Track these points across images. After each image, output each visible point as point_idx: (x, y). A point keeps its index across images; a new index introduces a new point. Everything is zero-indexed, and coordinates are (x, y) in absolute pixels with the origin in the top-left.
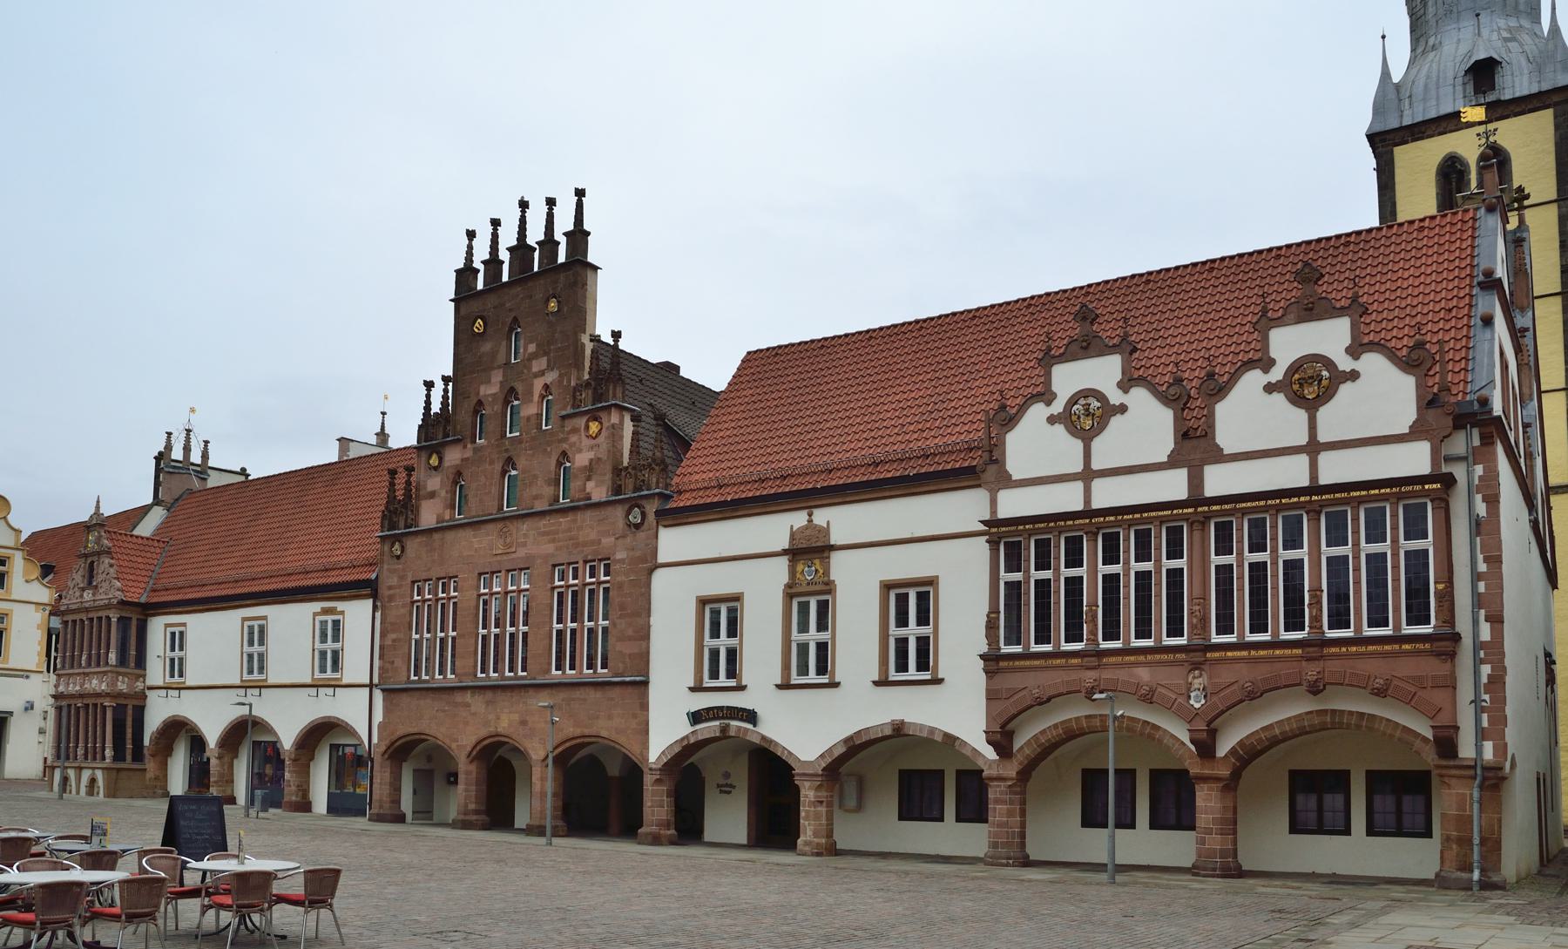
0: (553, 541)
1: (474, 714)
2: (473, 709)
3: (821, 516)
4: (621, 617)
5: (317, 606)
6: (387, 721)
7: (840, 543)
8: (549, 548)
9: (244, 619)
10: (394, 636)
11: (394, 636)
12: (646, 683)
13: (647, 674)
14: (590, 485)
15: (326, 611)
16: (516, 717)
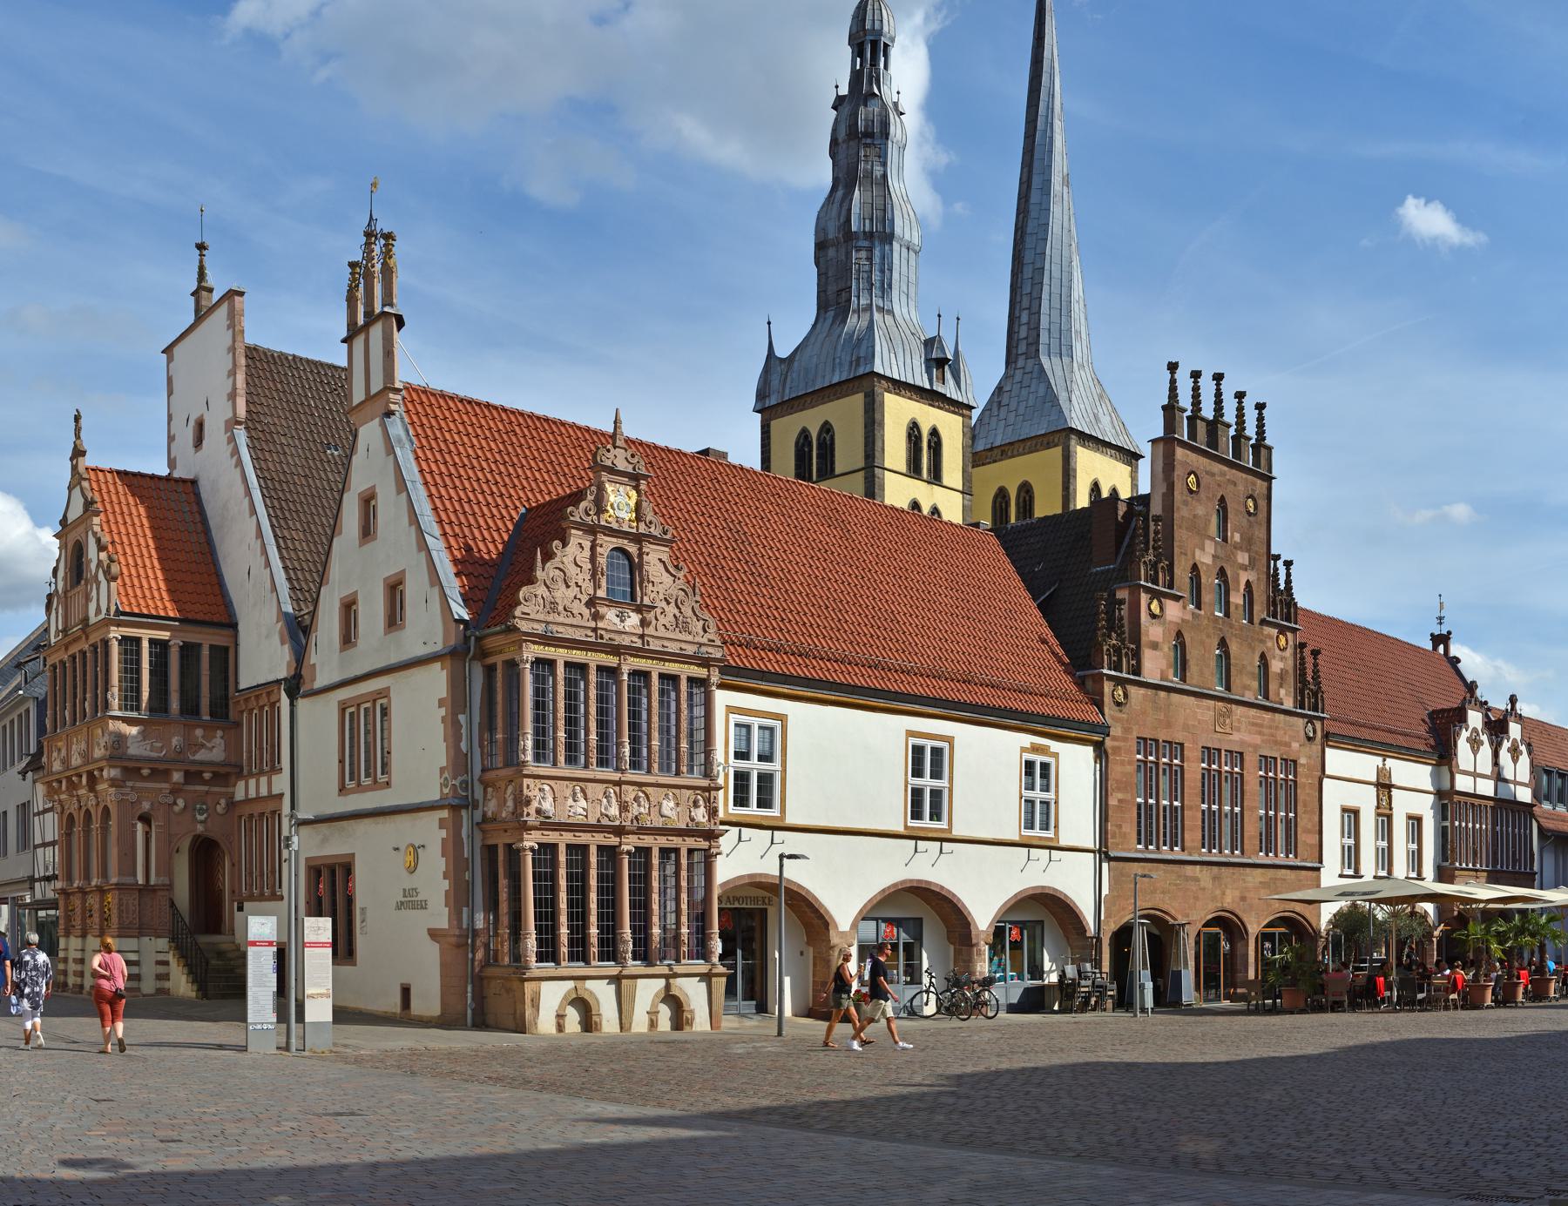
0: (1260, 733)
1: (1204, 889)
2: (1203, 884)
3: (1391, 763)
4: (1304, 813)
5: (1027, 739)
6: (1116, 894)
7: (1399, 784)
8: (1257, 739)
9: (910, 734)
10: (1120, 796)
11: (1120, 796)
12: (1318, 869)
13: (1321, 862)
14: (1282, 692)
15: (1035, 749)
16: (1237, 893)
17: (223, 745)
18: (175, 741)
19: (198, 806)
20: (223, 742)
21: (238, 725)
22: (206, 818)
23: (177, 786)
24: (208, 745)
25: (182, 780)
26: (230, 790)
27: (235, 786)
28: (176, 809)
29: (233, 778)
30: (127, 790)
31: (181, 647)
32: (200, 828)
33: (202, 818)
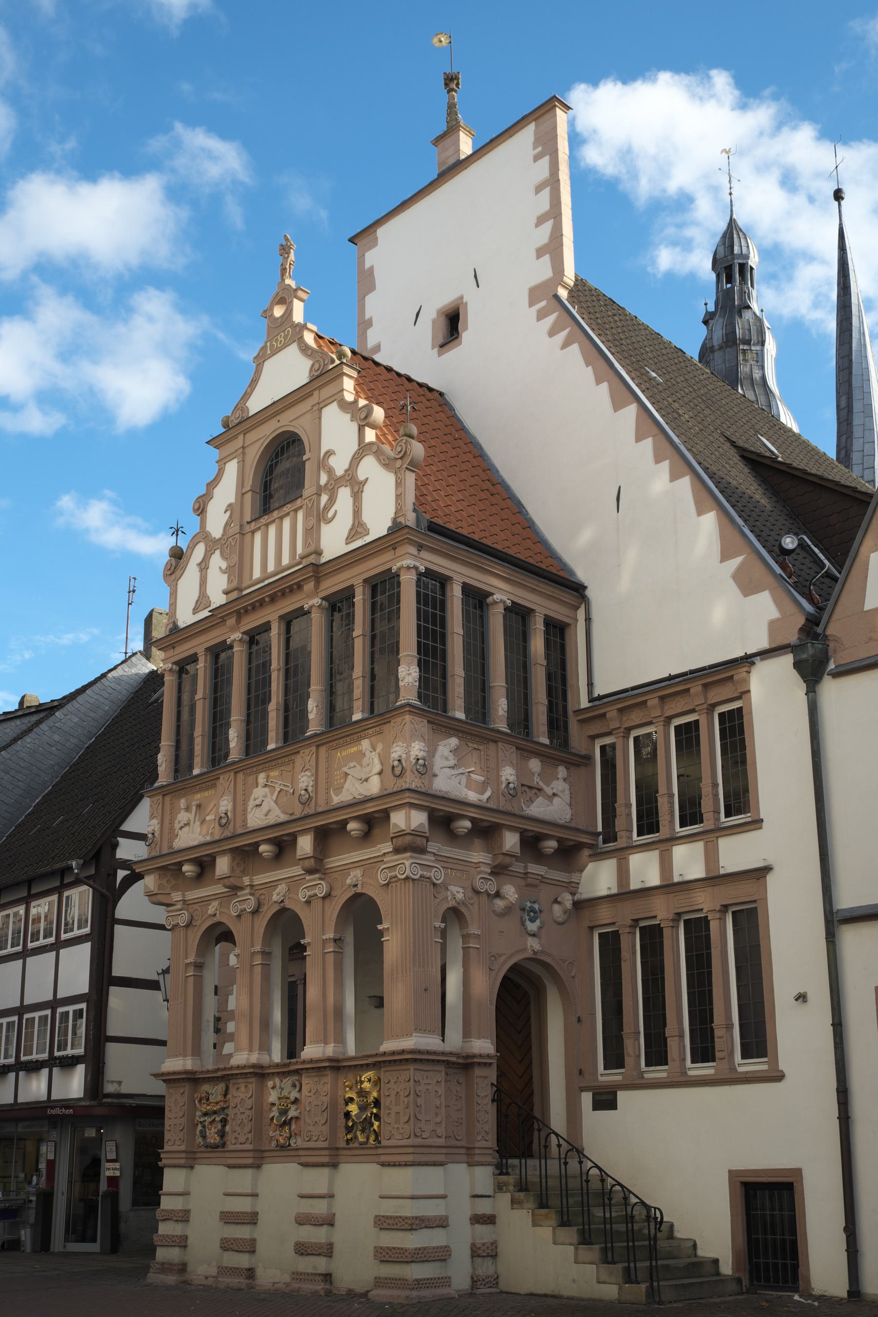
17: (567, 792)
18: (508, 773)
19: (529, 904)
20: (566, 786)
21: (588, 759)
22: (540, 928)
23: (508, 860)
24: (549, 791)
25: (517, 850)
26: (574, 878)
27: (581, 870)
28: (500, 904)
29: (586, 852)
30: (427, 860)
31: (507, 609)
32: (533, 944)
33: (532, 927)
